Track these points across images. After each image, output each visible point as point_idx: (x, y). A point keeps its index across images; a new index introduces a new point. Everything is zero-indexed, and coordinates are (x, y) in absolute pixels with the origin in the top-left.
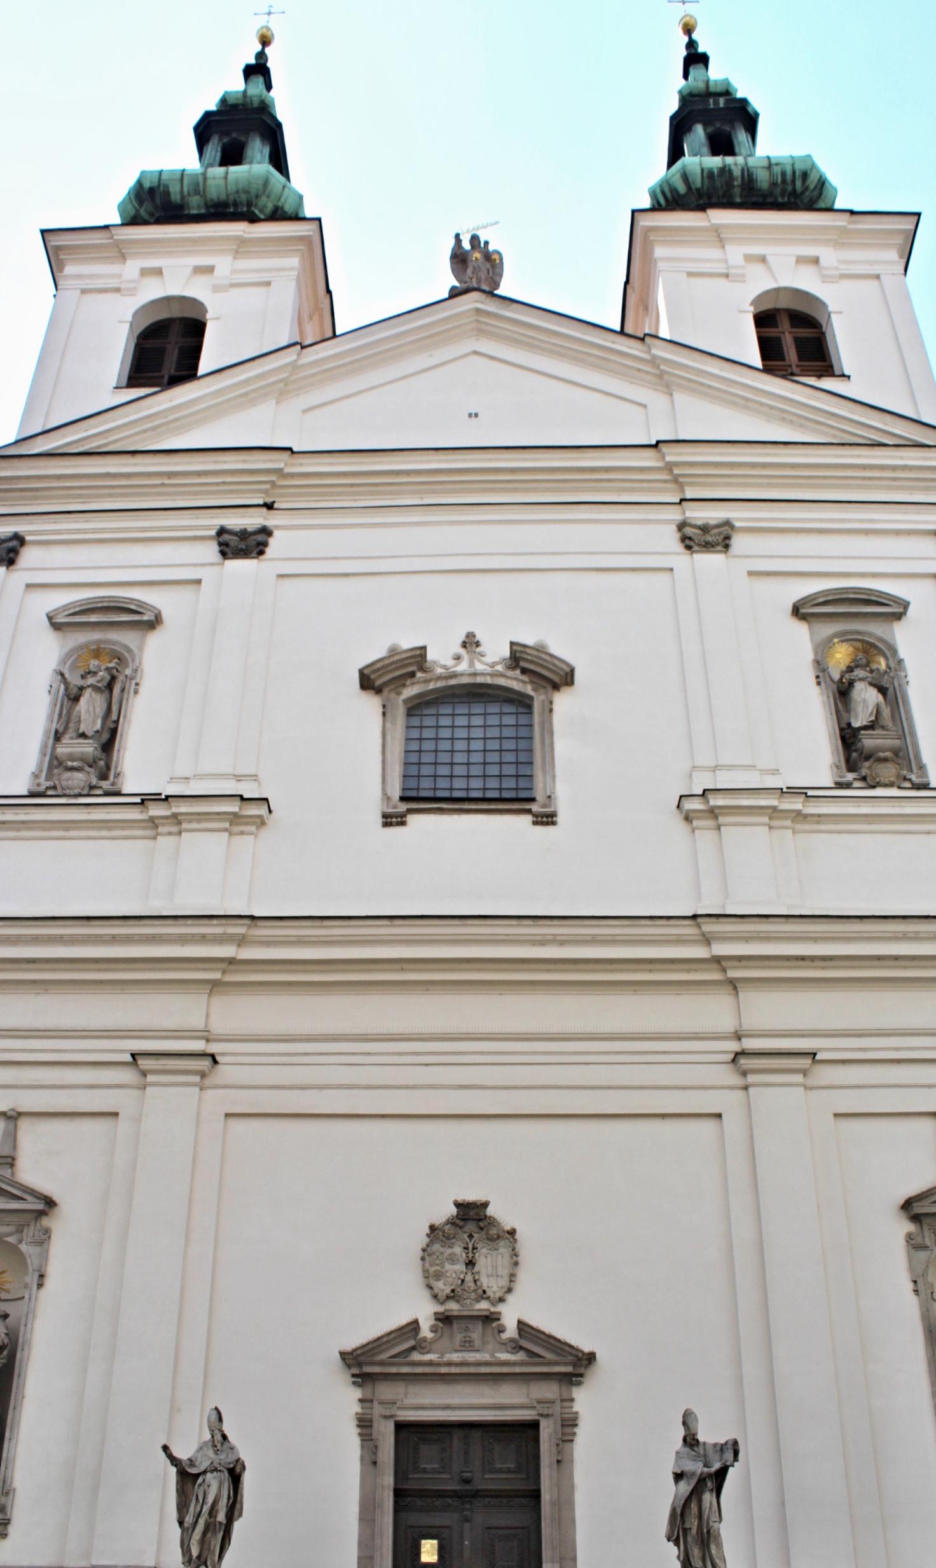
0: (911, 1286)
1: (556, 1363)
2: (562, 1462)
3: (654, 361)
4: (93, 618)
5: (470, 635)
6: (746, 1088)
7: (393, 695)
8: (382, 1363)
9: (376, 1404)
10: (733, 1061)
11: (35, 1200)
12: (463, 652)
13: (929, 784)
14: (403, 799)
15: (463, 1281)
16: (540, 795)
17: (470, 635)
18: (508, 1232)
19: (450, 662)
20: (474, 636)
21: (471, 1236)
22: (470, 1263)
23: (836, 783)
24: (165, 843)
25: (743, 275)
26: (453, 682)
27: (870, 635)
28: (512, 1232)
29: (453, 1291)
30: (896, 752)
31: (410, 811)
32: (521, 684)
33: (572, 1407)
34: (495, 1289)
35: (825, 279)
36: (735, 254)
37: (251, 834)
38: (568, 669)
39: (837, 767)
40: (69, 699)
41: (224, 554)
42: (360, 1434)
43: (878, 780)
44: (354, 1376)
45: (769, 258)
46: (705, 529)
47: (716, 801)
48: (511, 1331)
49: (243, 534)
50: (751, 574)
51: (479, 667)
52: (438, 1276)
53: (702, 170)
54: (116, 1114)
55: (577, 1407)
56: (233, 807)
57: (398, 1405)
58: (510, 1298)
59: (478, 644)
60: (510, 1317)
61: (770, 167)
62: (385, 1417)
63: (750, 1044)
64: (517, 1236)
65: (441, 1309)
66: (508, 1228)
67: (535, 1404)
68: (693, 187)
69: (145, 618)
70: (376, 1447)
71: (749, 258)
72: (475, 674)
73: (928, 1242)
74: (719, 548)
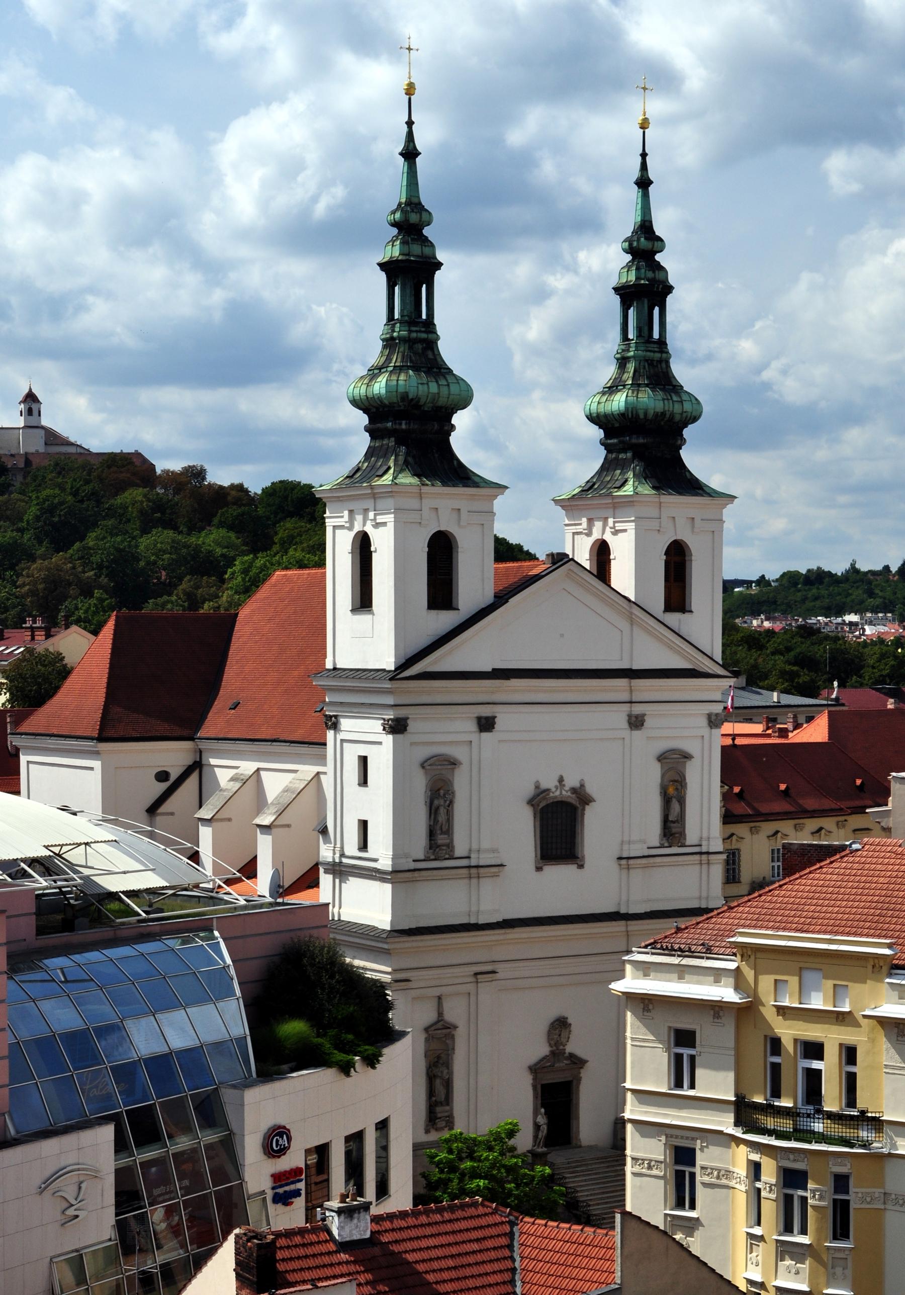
3: (631, 613)
12: (558, 784)
16: (580, 856)
22: (560, 1035)
26: (555, 800)
28: (570, 1024)
48: (567, 1055)
49: (487, 718)
52: (552, 1039)
55: (582, 1075)
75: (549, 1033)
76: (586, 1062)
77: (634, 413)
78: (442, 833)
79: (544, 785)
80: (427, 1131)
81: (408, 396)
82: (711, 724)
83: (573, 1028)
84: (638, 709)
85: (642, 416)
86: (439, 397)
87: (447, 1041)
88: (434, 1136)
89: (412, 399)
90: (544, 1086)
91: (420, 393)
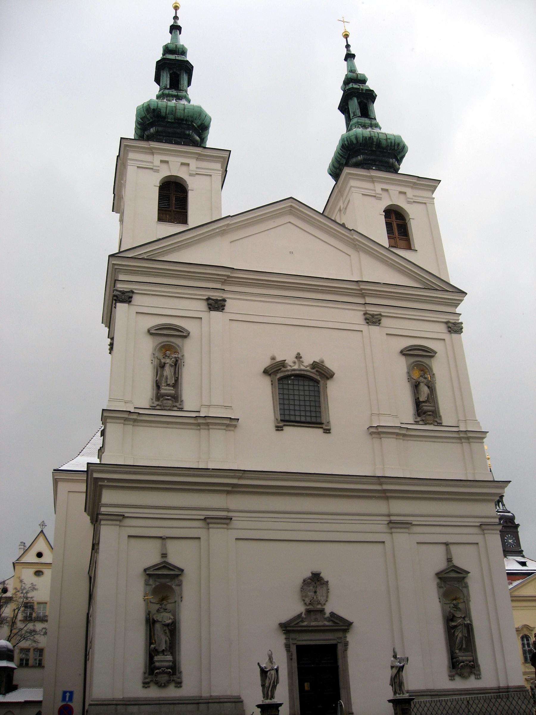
0: (438, 600)
1: (342, 626)
2: (345, 657)
3: (354, 239)
4: (165, 332)
5: (299, 354)
6: (391, 533)
7: (274, 376)
8: (293, 627)
9: (290, 639)
10: (388, 523)
11: (178, 571)
12: (296, 360)
13: (441, 423)
14: (281, 420)
15: (313, 598)
16: (324, 421)
17: (299, 354)
18: (326, 582)
19: (292, 364)
20: (300, 354)
21: (315, 583)
22: (315, 592)
23: (415, 422)
24: (204, 432)
25: (381, 198)
27: (425, 363)
28: (327, 582)
29: (310, 601)
30: (433, 412)
31: (285, 425)
32: (316, 376)
33: (346, 639)
34: (323, 600)
35: (409, 202)
36: (378, 187)
37: (233, 431)
38: (333, 374)
39: (415, 415)
40: (160, 367)
41: (210, 308)
42: (286, 650)
43: (427, 422)
44: (284, 630)
45: (390, 191)
46: (373, 316)
47: (380, 430)
48: (327, 615)
49: (216, 301)
50: (387, 334)
51: (302, 368)
52: (306, 596)
53: (363, 137)
54: (200, 538)
56: (227, 422)
57: (297, 640)
58: (327, 604)
59: (301, 357)
60: (328, 610)
61: (387, 139)
62: (294, 644)
63: (393, 518)
64: (329, 583)
65: (308, 607)
66: (326, 580)
67: (336, 639)
68: (359, 142)
69: (185, 334)
70: (292, 654)
71: (383, 189)
72: (301, 370)
73: (443, 586)
74: (377, 324)
75: (302, 589)
76: (352, 623)
77: (349, 140)
78: (168, 385)
79: (279, 358)
80: (146, 685)
81: (150, 108)
82: (450, 329)
83: (331, 585)
84: (372, 310)
85: (355, 141)
86: (176, 109)
87: (174, 587)
88: (153, 693)
89: (154, 110)
90: (301, 649)
91: (159, 105)
